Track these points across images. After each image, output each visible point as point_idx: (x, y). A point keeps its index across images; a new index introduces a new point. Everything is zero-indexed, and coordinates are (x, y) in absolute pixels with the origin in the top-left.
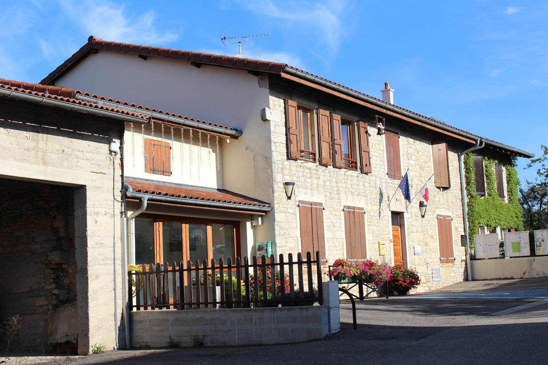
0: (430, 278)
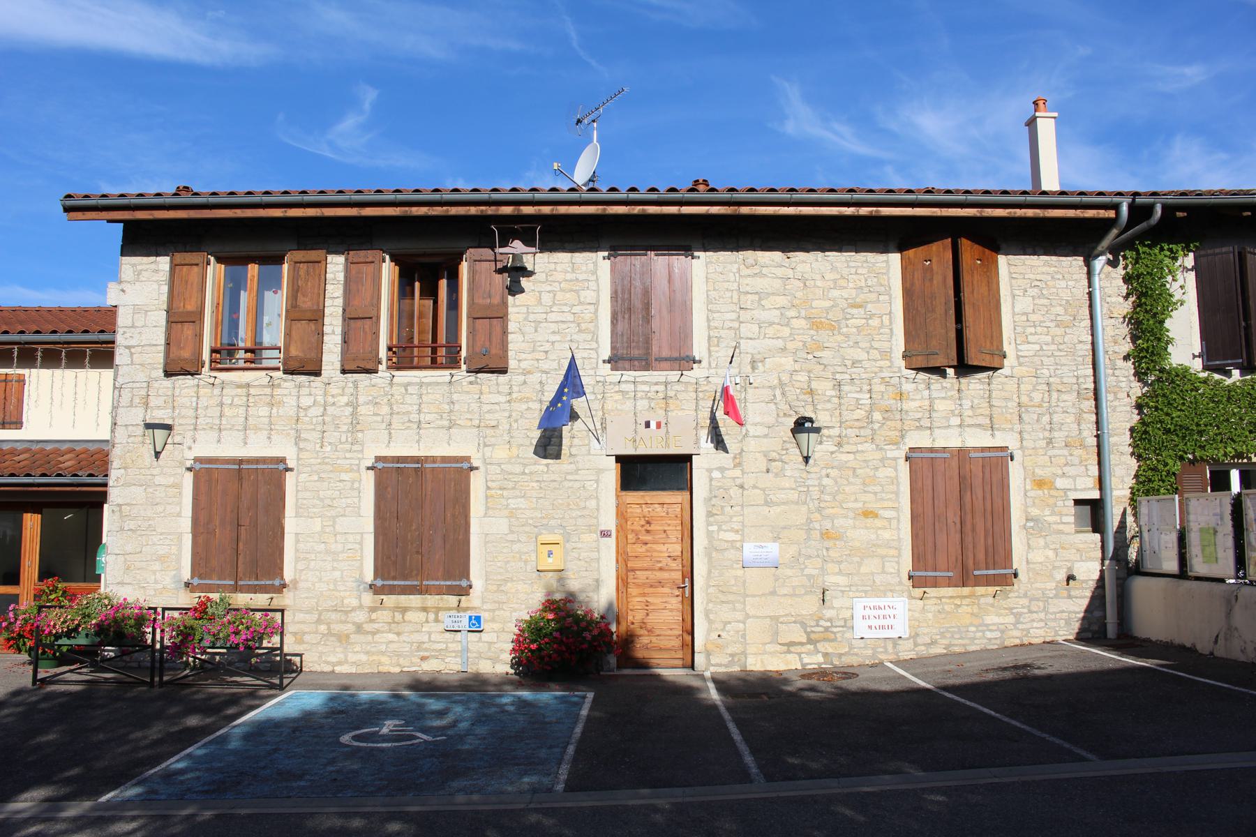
0: (835, 630)
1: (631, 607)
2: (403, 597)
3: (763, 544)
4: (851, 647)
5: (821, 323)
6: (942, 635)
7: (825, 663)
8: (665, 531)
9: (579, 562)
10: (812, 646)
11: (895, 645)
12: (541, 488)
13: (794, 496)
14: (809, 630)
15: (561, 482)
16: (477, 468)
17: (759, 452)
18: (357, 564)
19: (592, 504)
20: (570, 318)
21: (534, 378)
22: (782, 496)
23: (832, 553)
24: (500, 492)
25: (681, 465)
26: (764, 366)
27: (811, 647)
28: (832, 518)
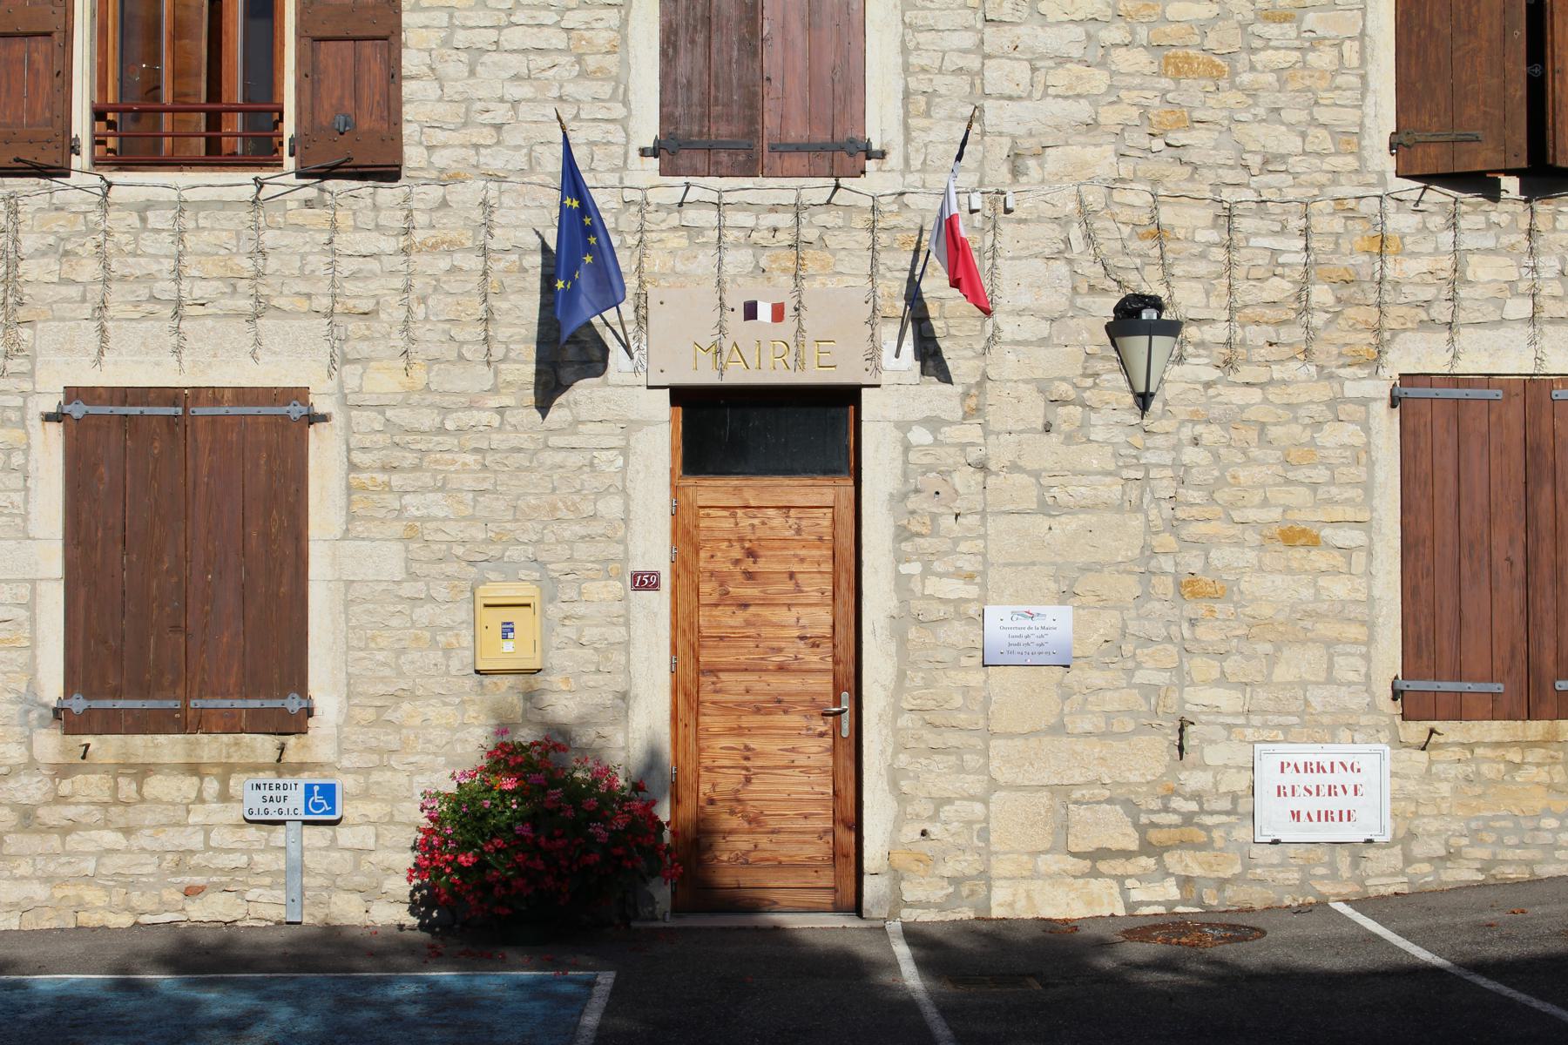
0: (1208, 820)
1: (708, 762)
2: (139, 740)
3: (1034, 609)
4: (1248, 862)
5: (1187, 59)
6: (1475, 837)
7: (1184, 902)
8: (792, 575)
9: (579, 652)
10: (1152, 861)
11: (1357, 860)
12: (485, 466)
13: (1111, 490)
14: (1144, 819)
15: (535, 452)
16: (324, 418)
17: (1026, 382)
18: (22, 658)
19: (611, 507)
20: (559, 40)
21: (468, 193)
22: (1081, 490)
23: (1201, 631)
24: (381, 477)
25: (833, 411)
26: (1041, 166)
27: (1148, 862)
28: (1203, 545)
